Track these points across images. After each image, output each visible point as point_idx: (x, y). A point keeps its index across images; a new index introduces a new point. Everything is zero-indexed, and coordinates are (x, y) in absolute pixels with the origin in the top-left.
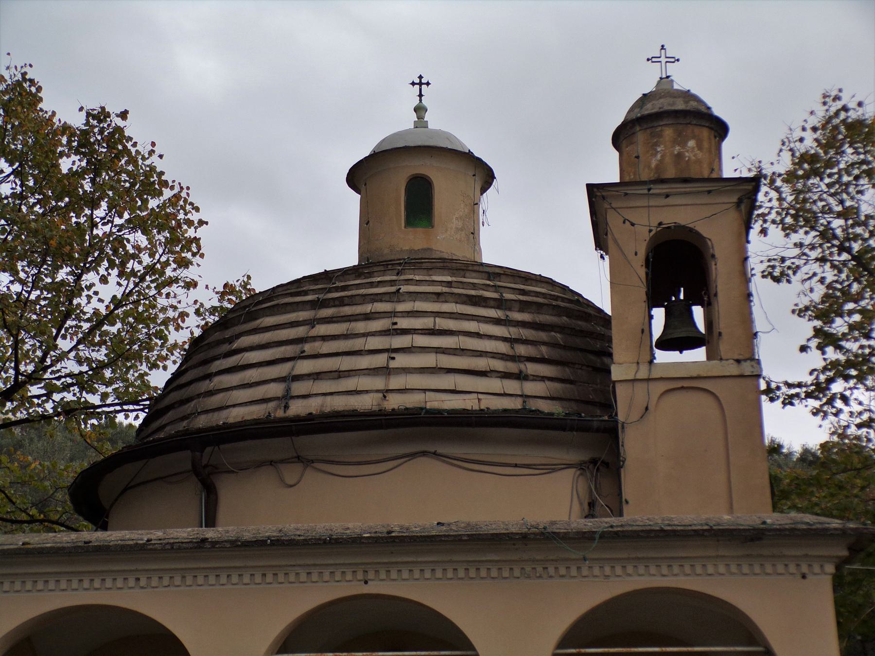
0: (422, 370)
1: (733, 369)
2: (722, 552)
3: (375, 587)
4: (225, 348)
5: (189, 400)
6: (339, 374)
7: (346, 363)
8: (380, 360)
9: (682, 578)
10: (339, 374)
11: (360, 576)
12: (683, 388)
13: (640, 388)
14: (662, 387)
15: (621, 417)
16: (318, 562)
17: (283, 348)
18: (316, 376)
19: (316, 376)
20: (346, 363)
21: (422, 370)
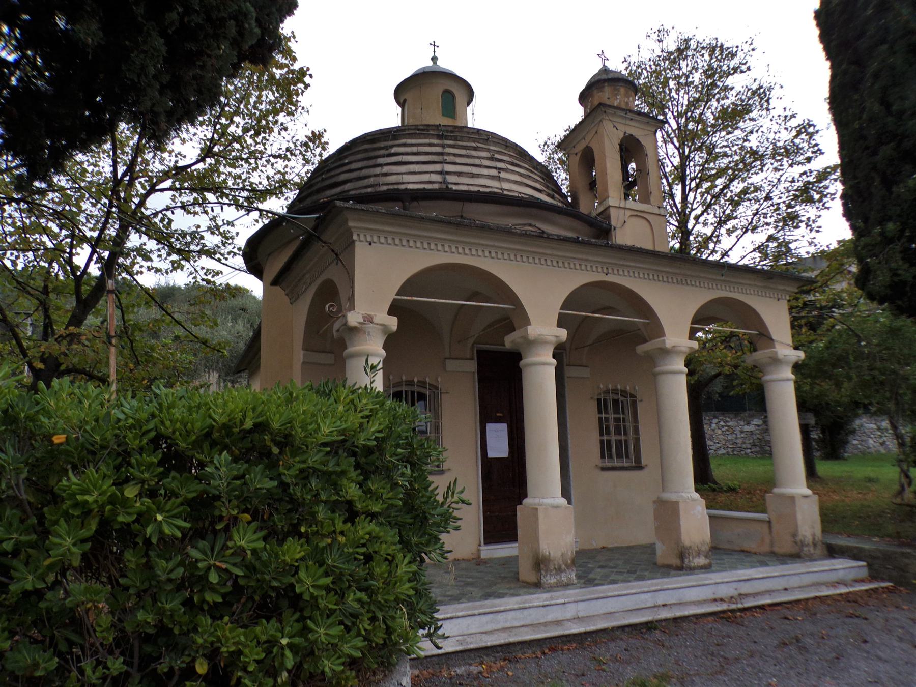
0: (515, 182)
1: (656, 211)
2: (756, 283)
3: (611, 278)
4: (382, 152)
5: (369, 177)
6: (473, 176)
7: (475, 170)
8: (494, 172)
9: (737, 294)
10: (473, 176)
11: (605, 271)
12: (637, 216)
13: (622, 211)
14: (629, 213)
15: (613, 223)
16: (591, 258)
17: (430, 156)
18: (460, 174)
19: (460, 174)
20: (475, 170)
21: (515, 182)
